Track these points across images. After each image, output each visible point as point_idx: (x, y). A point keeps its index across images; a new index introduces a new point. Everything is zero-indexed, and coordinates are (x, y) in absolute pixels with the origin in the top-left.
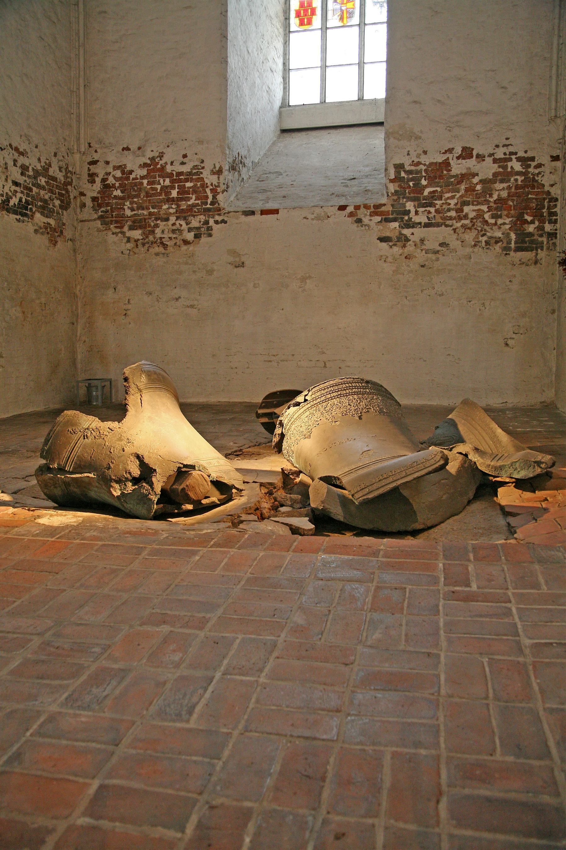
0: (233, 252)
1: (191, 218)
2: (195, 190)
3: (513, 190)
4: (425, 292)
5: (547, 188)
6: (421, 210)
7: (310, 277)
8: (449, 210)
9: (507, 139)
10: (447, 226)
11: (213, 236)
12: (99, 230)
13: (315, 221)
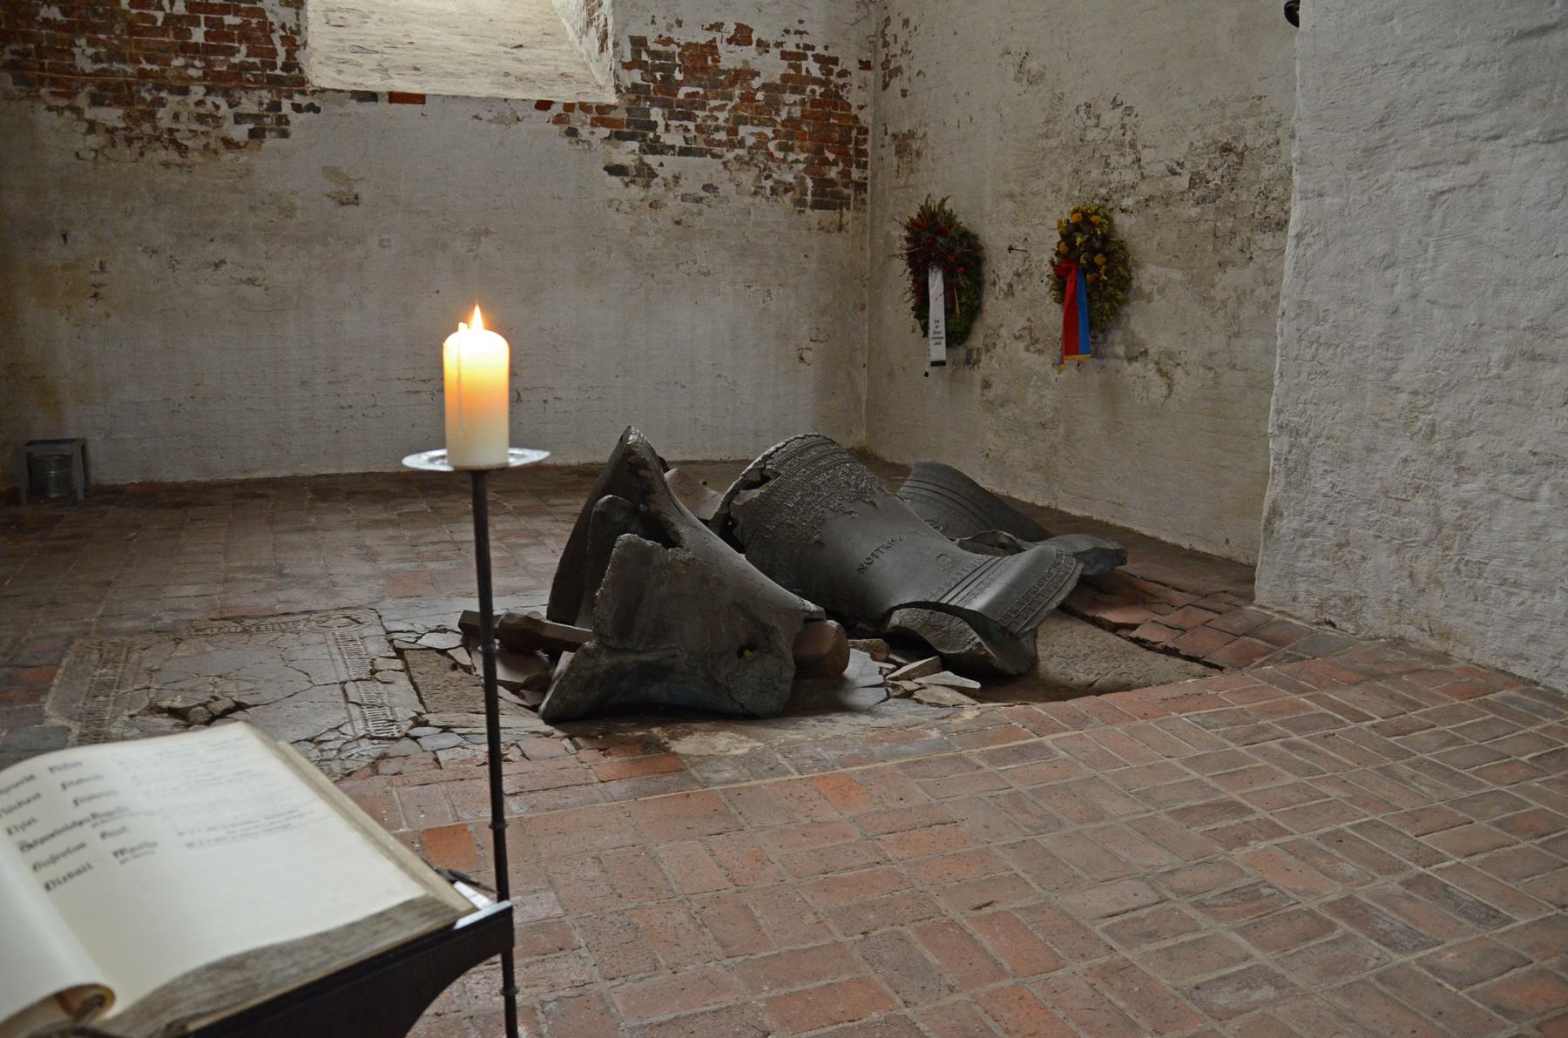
0: (333, 173)
1: (238, 94)
2: (245, 34)
3: (808, 107)
5: (854, 111)
6: (674, 123)
7: (487, 232)
8: (717, 129)
9: (801, 22)
10: (714, 156)
11: (293, 136)
12: (9, 97)
13: (493, 125)
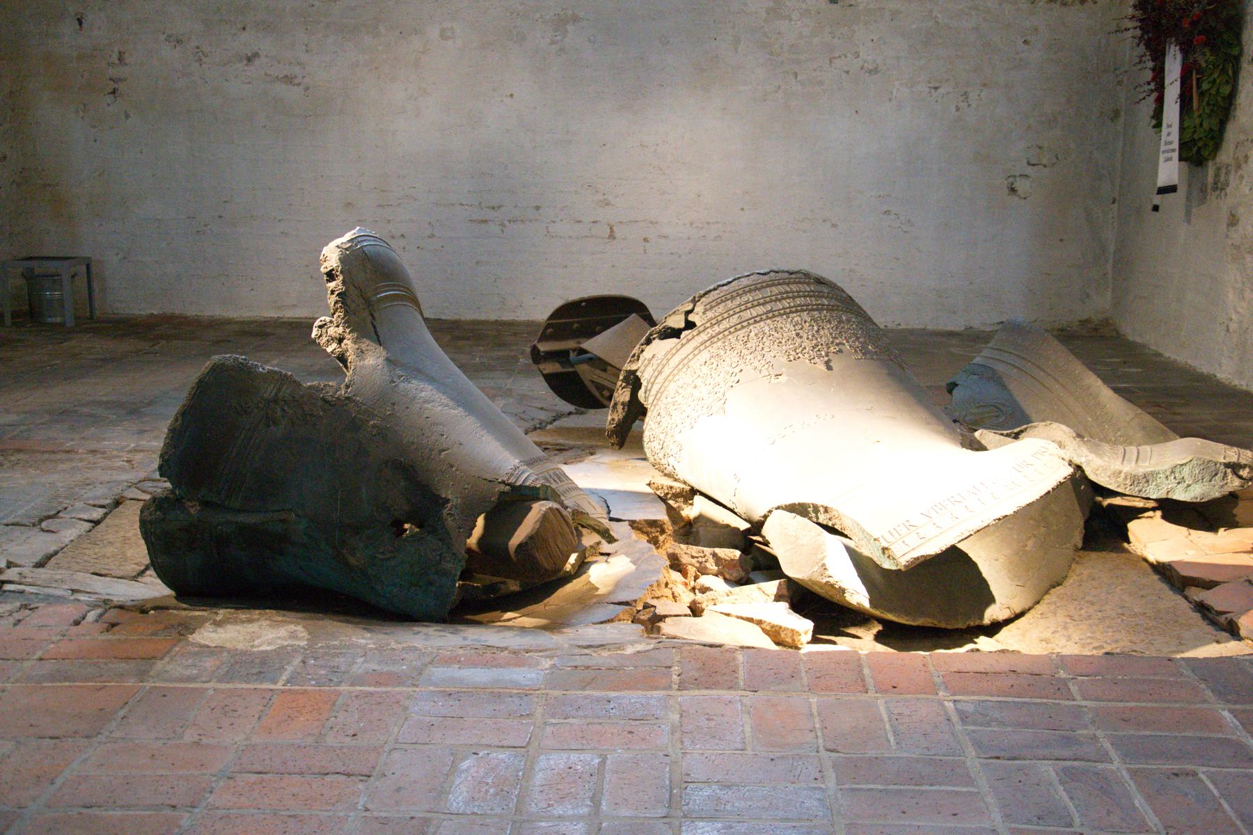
4: (838, 62)
7: (575, 19)
